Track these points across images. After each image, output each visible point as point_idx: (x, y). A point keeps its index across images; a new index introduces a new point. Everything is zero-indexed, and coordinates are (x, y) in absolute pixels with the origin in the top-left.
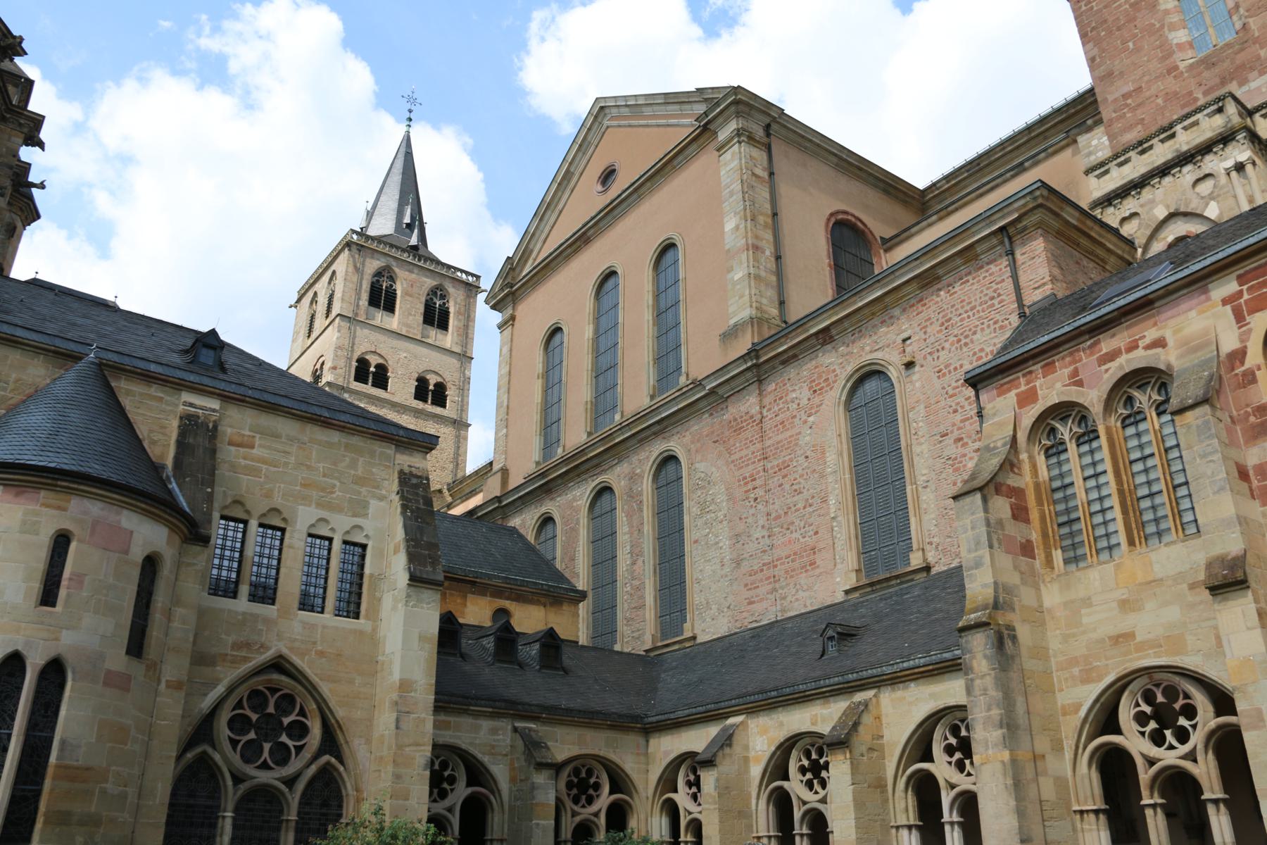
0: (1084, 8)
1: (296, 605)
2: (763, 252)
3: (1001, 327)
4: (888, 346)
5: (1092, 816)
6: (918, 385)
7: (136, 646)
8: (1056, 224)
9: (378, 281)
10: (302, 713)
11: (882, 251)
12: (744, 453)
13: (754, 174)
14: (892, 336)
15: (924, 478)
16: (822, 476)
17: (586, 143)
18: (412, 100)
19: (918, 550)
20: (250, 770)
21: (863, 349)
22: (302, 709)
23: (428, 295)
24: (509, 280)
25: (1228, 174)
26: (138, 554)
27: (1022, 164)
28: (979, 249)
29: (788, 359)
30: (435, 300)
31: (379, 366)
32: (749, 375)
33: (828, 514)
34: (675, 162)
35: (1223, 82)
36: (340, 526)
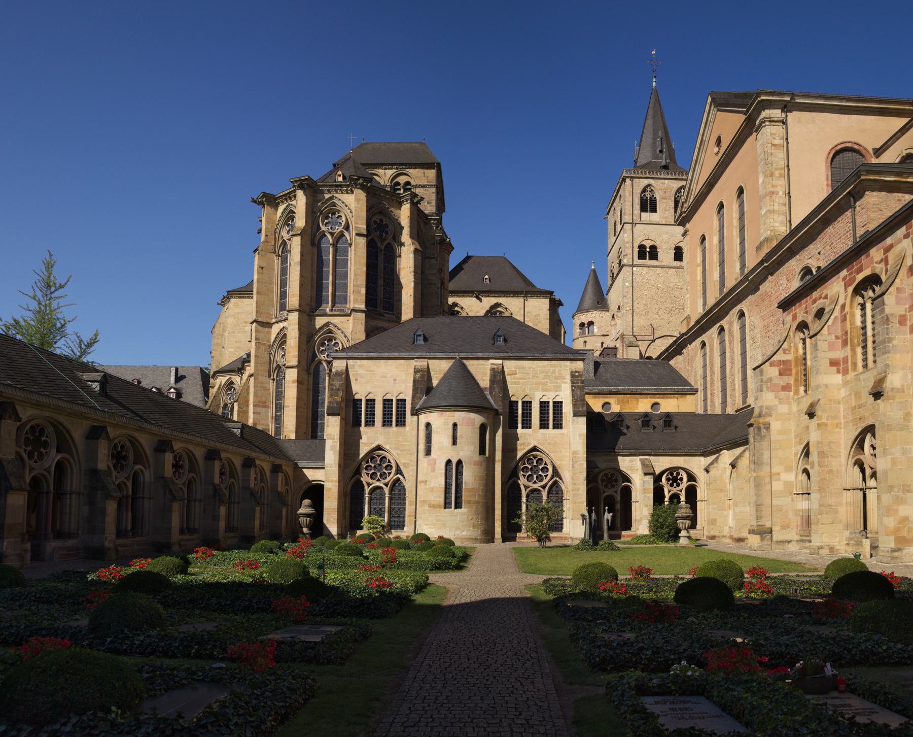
1: (538, 427)
9: (644, 195)
10: (546, 464)
20: (530, 484)
23: (676, 194)
24: (683, 210)
26: (478, 425)
36: (550, 398)
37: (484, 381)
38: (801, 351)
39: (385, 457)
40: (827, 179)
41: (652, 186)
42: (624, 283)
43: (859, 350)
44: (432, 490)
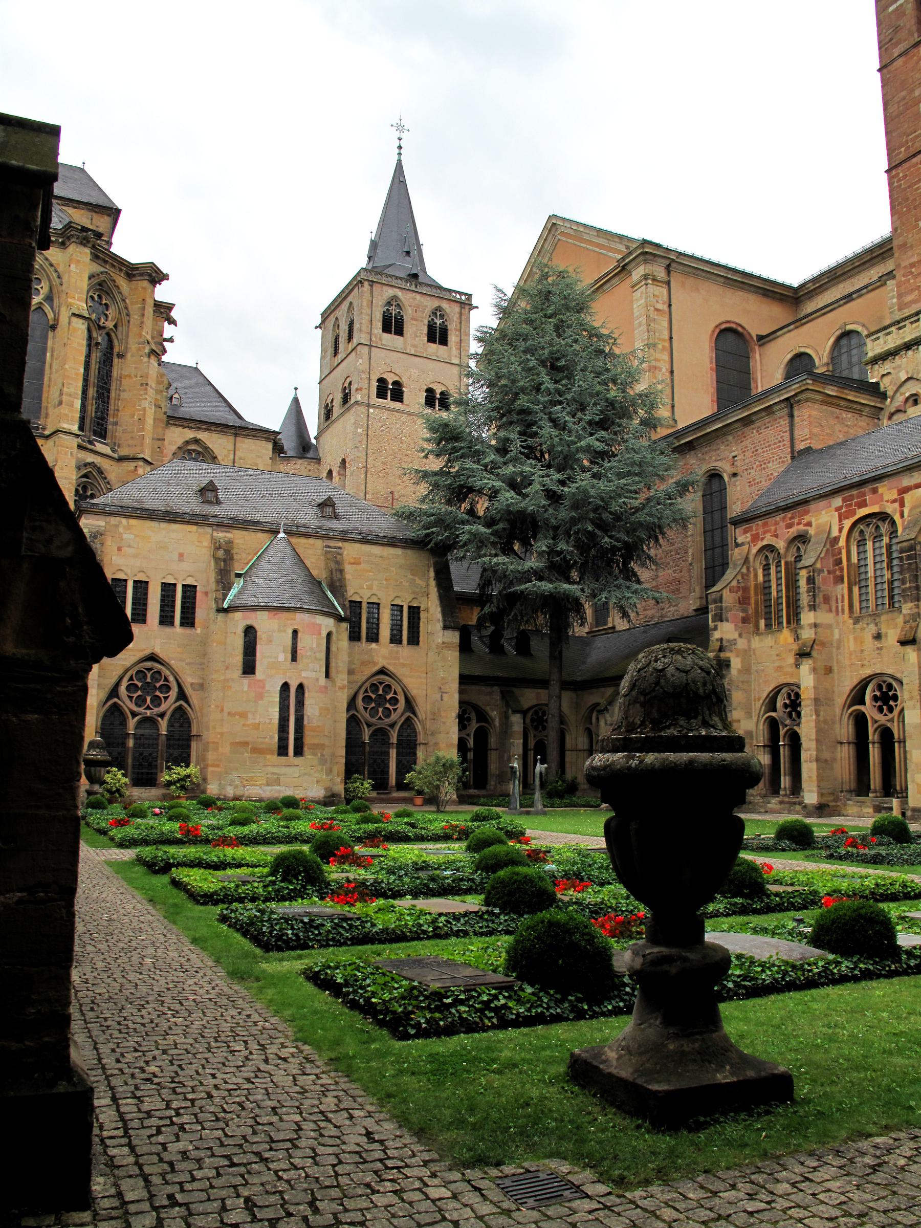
0: (896, 184)
2: (660, 370)
3: (783, 462)
5: (762, 749)
6: (739, 488)
7: (327, 675)
8: (819, 397)
10: (395, 693)
11: (757, 347)
13: (657, 310)
14: (727, 453)
16: (686, 537)
17: (544, 250)
18: (400, 128)
26: (324, 634)
27: (850, 295)
30: (436, 320)
31: (396, 383)
33: (687, 560)
34: (605, 287)
37: (319, 571)
38: (761, 578)
39: (159, 672)
40: (711, 362)
42: (357, 428)
43: (856, 590)
44: (257, 726)
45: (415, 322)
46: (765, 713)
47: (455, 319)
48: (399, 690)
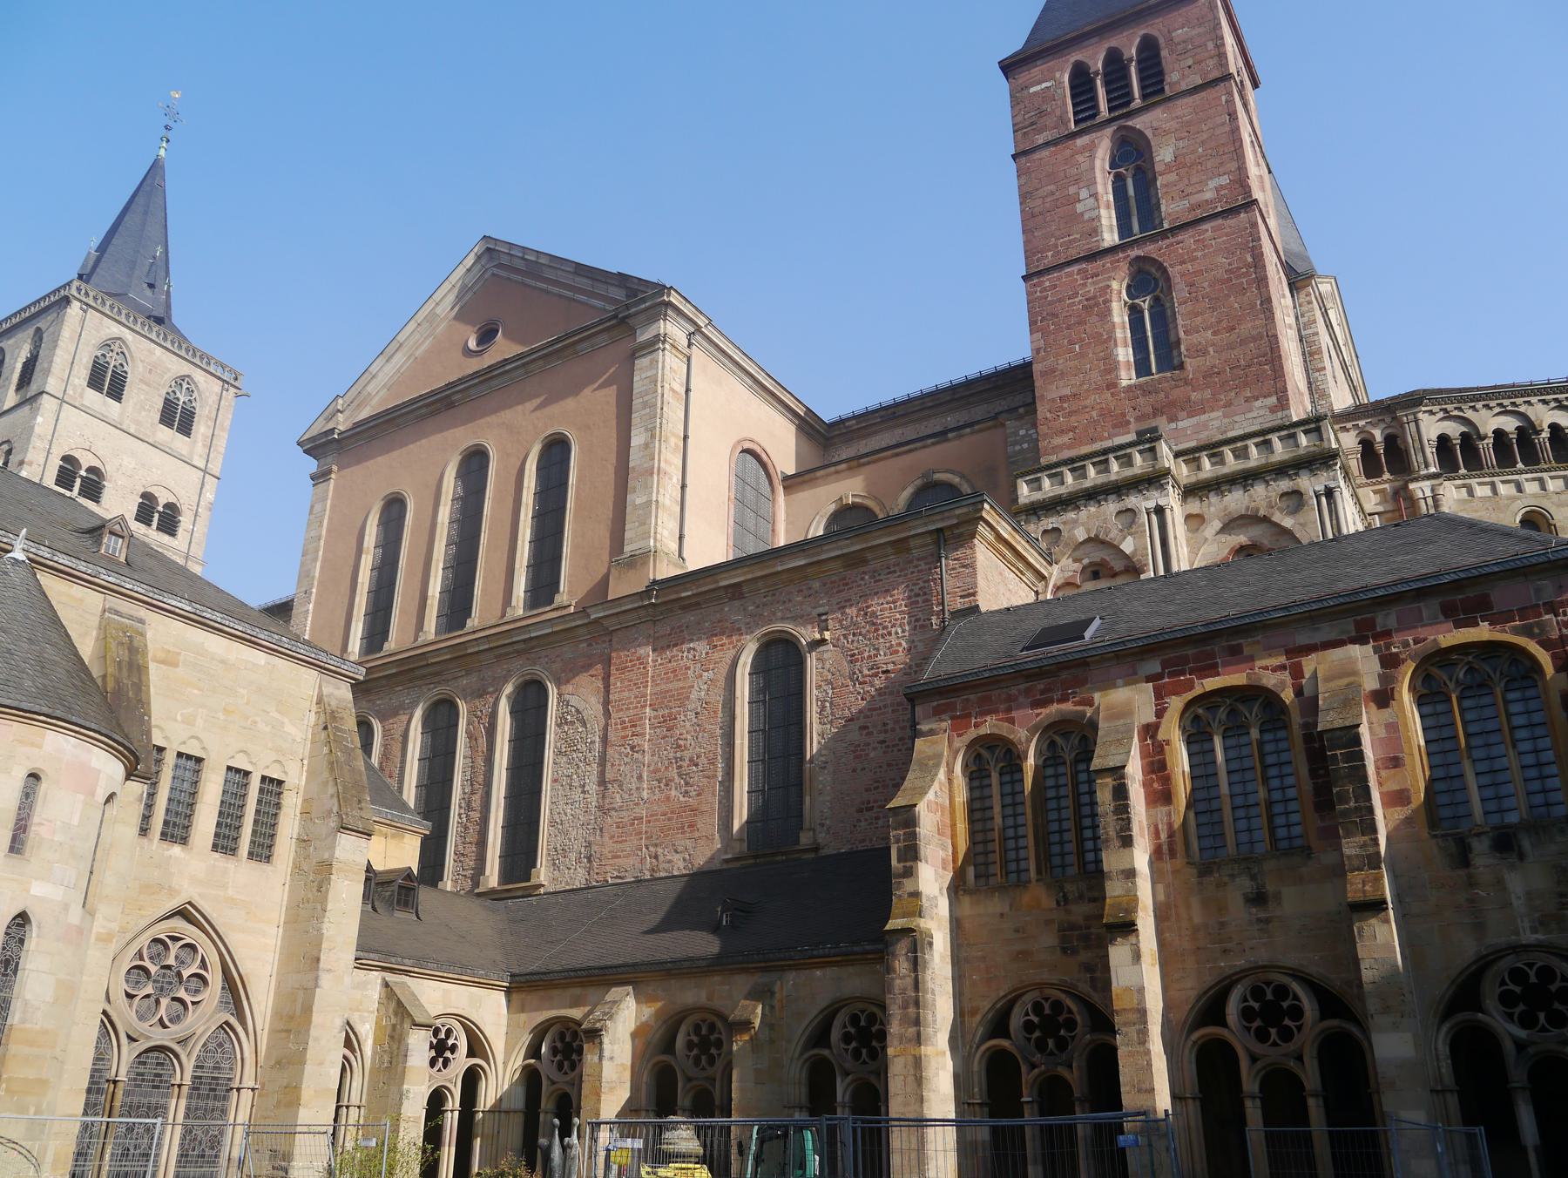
2: (671, 479)
4: (802, 617)
5: (977, 1108)
10: (204, 965)
12: (626, 694)
13: (672, 390)
15: (823, 759)
19: (810, 829)
20: (143, 1027)
21: (774, 614)
22: (203, 960)
25: (1148, 514)
26: (101, 796)
28: (912, 543)
29: (688, 606)
30: (178, 394)
31: (91, 470)
32: (643, 612)
35: (1156, 412)
41: (127, 346)
45: (144, 387)
46: (982, 1042)
47: (210, 402)
48: (213, 959)
